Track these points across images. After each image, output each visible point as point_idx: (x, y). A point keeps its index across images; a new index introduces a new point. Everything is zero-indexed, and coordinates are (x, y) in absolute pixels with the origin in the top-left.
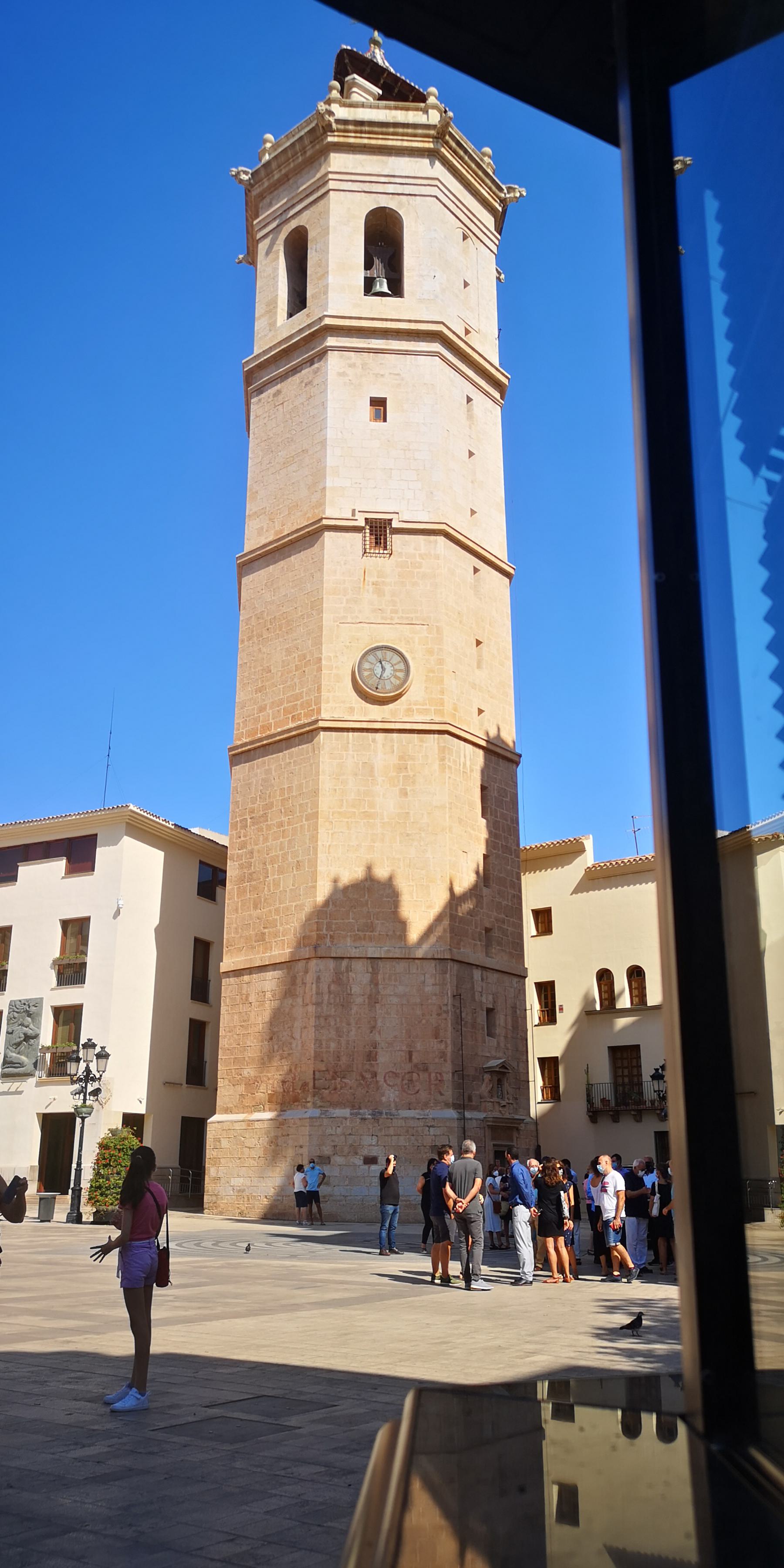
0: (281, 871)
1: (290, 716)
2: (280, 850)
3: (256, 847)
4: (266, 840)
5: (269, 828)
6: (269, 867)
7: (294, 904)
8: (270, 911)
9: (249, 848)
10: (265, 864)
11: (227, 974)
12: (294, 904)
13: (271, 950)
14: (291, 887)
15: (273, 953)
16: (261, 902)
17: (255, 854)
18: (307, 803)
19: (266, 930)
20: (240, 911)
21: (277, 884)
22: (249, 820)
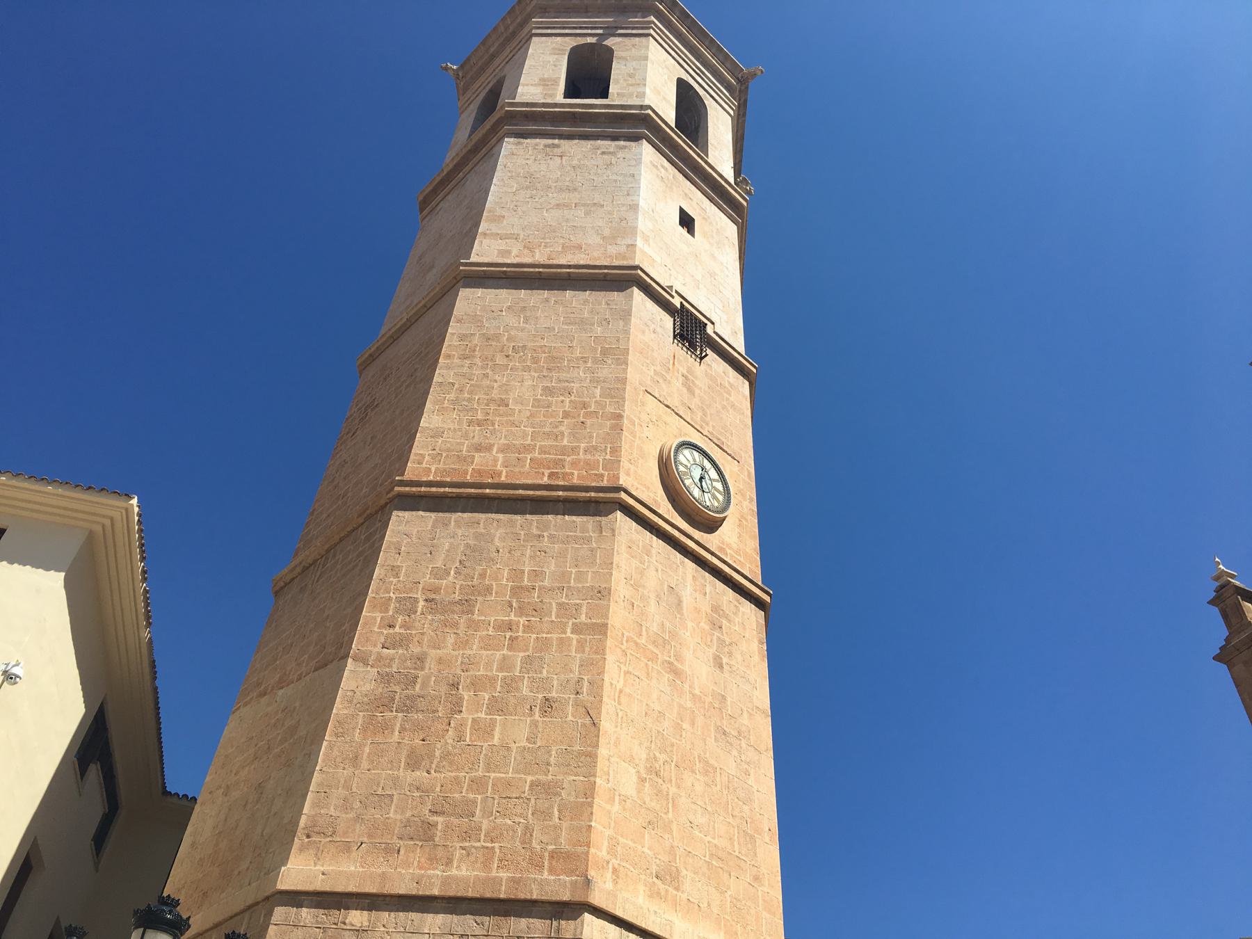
0: (497, 707)
1: (547, 472)
2: (501, 669)
3: (433, 653)
4: (463, 644)
5: (474, 625)
6: (466, 695)
7: (529, 778)
8: (457, 781)
9: (416, 650)
10: (455, 686)
11: (296, 898)
12: (529, 778)
13: (449, 862)
14: (524, 743)
15: (454, 872)
16: (431, 756)
17: (431, 665)
18: (579, 605)
19: (440, 819)
20: (365, 764)
21: (484, 730)
22: (422, 603)
